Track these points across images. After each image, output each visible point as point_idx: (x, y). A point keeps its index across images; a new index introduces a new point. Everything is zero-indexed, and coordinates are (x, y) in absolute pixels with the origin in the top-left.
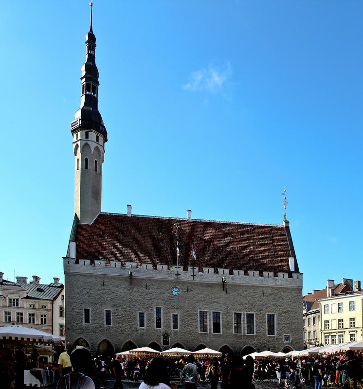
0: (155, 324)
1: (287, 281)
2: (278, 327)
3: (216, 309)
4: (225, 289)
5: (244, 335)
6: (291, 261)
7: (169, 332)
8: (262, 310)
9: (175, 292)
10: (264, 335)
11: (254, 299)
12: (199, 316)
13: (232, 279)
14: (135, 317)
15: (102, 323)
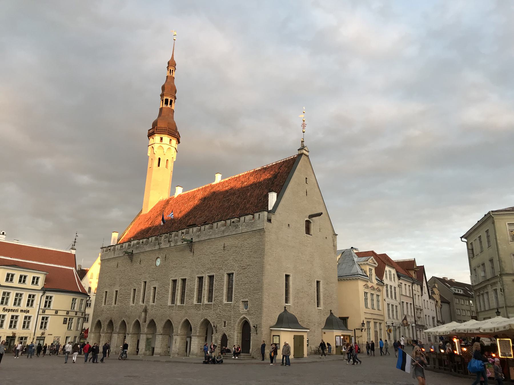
0: (141, 300)
1: (247, 225)
2: (236, 289)
3: (183, 275)
4: (193, 250)
5: (203, 305)
6: (273, 197)
7: (148, 308)
8: (221, 269)
9: (158, 263)
10: (221, 302)
11: (215, 257)
12: (170, 286)
13: (198, 236)
14: (130, 294)
15: (112, 304)
